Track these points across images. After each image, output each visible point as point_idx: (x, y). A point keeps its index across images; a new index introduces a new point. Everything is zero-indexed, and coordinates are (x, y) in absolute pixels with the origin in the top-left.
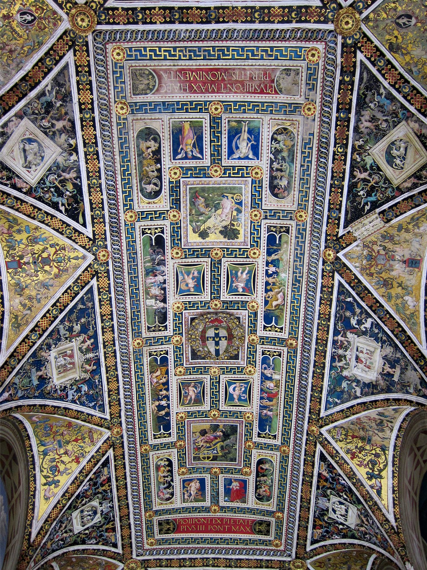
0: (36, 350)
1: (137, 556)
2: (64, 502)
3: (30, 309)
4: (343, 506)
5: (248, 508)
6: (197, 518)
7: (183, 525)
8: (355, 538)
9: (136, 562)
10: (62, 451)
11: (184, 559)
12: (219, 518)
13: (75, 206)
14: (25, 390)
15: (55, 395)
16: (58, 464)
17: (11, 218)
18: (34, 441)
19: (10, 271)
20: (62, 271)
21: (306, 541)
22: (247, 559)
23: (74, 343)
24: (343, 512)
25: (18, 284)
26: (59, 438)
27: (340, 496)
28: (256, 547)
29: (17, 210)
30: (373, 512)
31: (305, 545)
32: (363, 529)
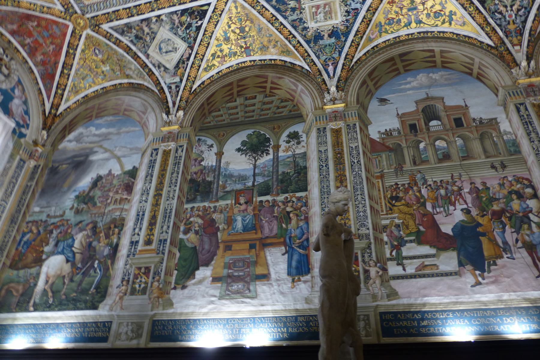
0: (305, 40)
2: (472, 9)
3: (277, 42)
10: (421, 7)
13: (196, 13)
14: (335, 50)
15: (351, 21)
16: (434, 10)
17: (211, 58)
18: (403, 32)
19: (252, 54)
20: (248, 18)
23: (306, 6)
25: (261, 49)
26: (405, 11)
29: (203, 56)
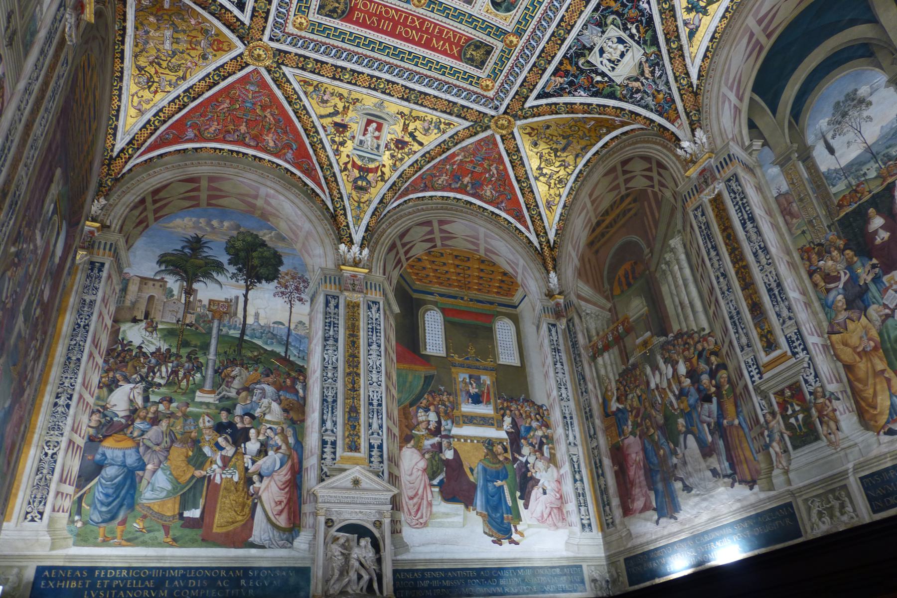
1: (271, 39)
4: (621, 47)
5: (470, 15)
6: (385, 6)
7: (360, 10)
8: (615, 98)
9: (266, 49)
11: (343, 69)
12: (419, 18)
21: (532, 91)
22: (435, 97)
24: (616, 56)
27: (625, 29)
28: (455, 82)
30: (671, 59)
31: (527, 98)
32: (637, 84)
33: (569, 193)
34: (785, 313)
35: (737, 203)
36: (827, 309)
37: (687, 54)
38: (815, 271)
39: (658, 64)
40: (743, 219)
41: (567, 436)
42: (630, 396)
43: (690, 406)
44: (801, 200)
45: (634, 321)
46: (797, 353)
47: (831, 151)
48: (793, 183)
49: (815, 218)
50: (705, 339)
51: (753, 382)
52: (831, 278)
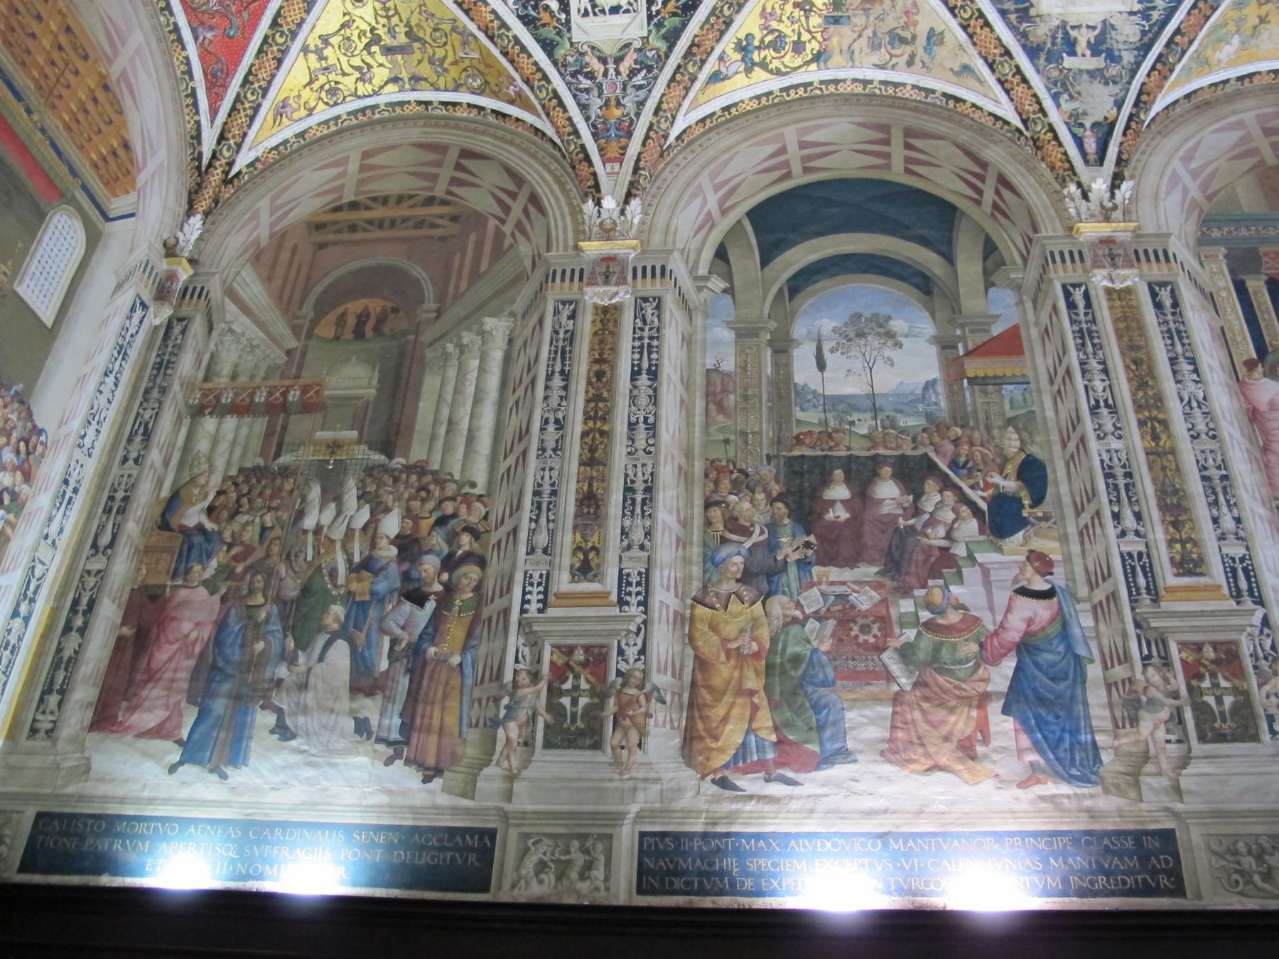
8: (550, 55)
32: (597, 67)
33: (326, 122)
34: (638, 536)
35: (641, 338)
36: (709, 565)
37: (691, 95)
38: (717, 503)
39: (650, 68)
40: (639, 366)
41: (50, 519)
42: (243, 518)
43: (373, 594)
44: (746, 398)
45: (333, 398)
46: (628, 603)
47: (821, 365)
48: (744, 368)
49: (753, 433)
50: (467, 500)
51: (523, 611)
52: (735, 526)
